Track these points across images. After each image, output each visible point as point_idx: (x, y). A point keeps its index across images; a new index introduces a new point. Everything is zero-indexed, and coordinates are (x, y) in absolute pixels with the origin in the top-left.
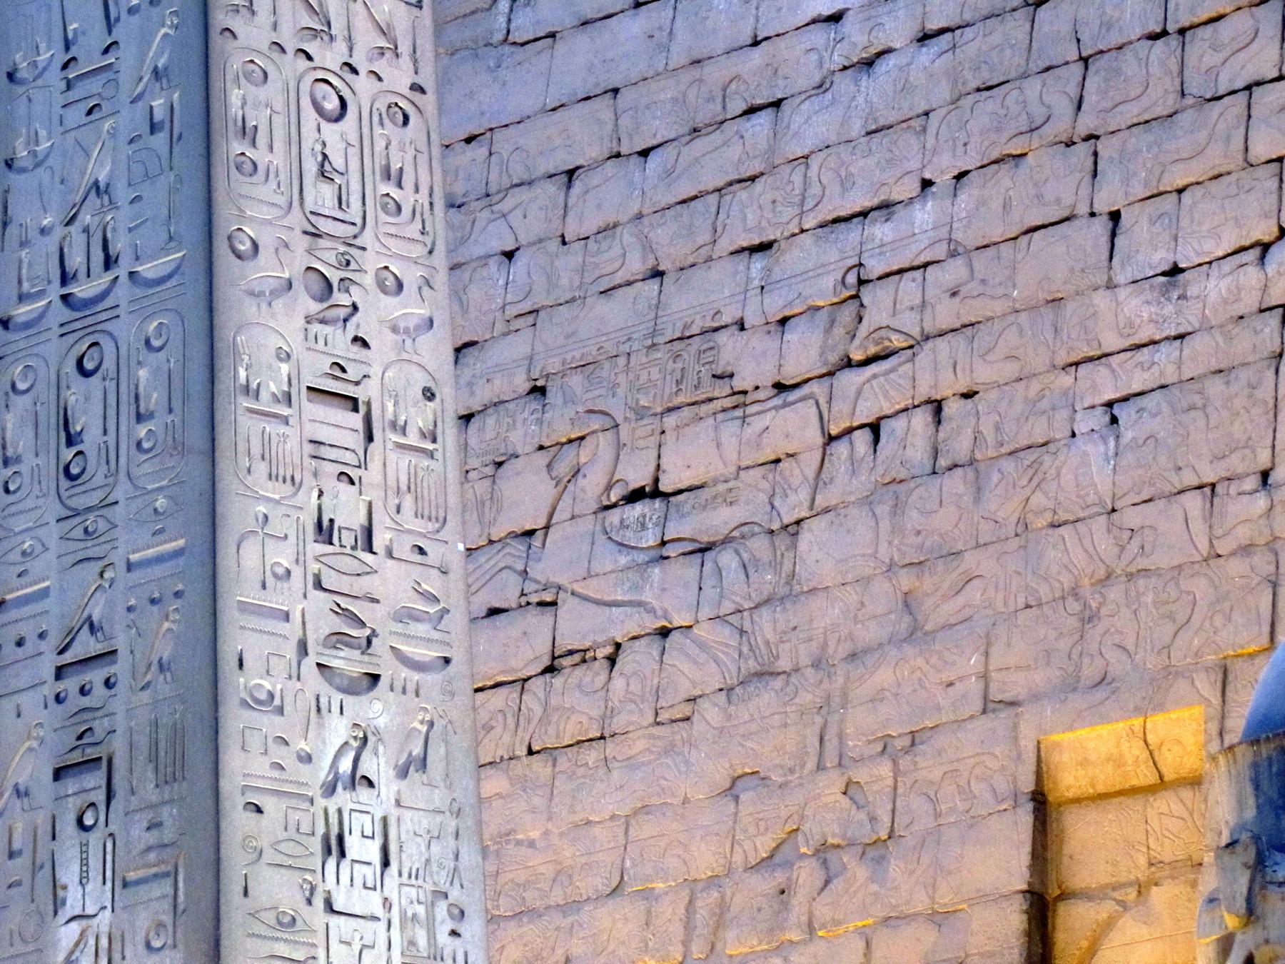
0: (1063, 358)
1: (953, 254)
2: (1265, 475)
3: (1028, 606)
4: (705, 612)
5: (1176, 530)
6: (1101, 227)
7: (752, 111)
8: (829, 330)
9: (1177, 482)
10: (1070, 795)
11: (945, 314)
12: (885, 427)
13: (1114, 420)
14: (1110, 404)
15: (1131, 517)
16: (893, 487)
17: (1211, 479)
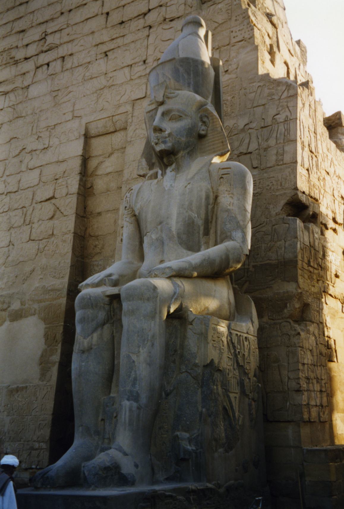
0: (94, 44)
1: (68, 26)
2: (144, 62)
3: (84, 96)
4: (6, 105)
5: (122, 76)
6: (105, 16)
7: (21, 4)
8: (38, 45)
9: (122, 66)
10: (92, 135)
11: (66, 39)
12: (50, 64)
13: (107, 55)
14: (105, 52)
15: (110, 75)
16: (52, 76)
17: (131, 64)
